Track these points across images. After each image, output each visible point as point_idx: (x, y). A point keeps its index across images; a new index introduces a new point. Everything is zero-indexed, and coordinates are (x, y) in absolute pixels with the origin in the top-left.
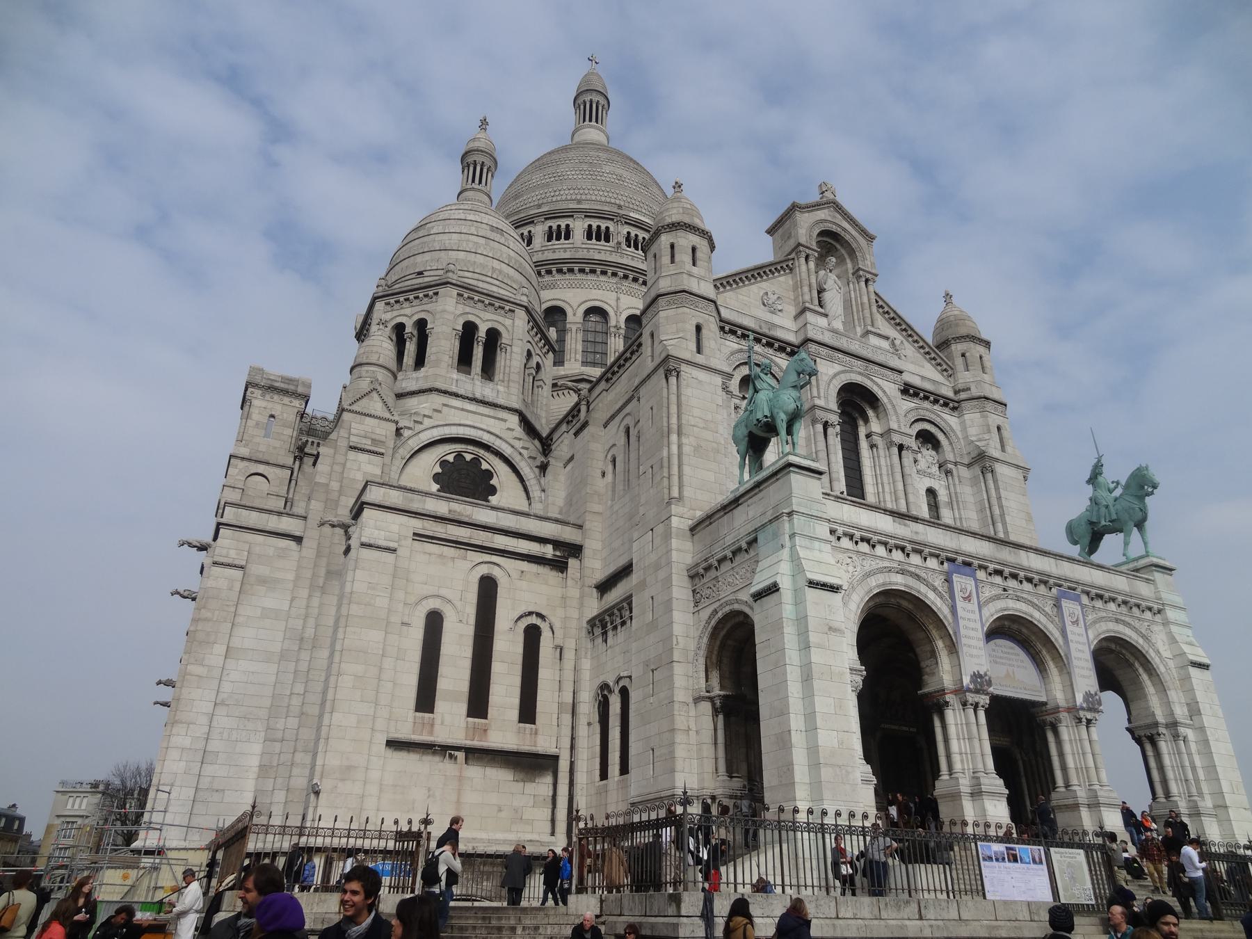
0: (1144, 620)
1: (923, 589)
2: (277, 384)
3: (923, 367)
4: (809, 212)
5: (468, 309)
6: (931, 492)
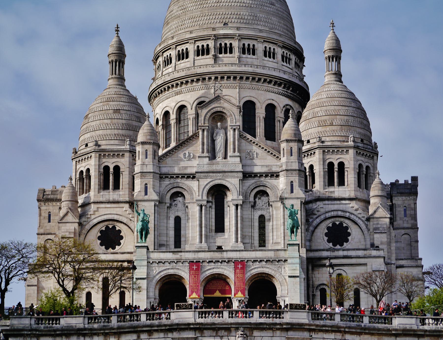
0: (277, 265)
2: (49, 197)
3: (266, 159)
4: (205, 107)
5: (104, 160)
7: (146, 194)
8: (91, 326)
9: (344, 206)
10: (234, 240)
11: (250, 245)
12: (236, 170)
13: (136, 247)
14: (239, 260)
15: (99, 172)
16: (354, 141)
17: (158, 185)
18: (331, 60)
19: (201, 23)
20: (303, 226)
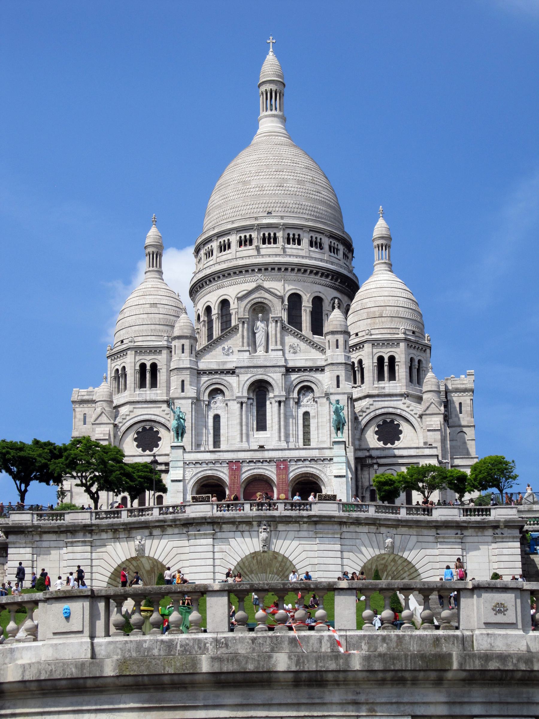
1: (219, 473)
3: (310, 352)
5: (141, 357)
6: (306, 414)
7: (183, 391)
8: (98, 522)
9: (395, 402)
10: (277, 439)
11: (293, 444)
12: (278, 364)
13: (171, 447)
14: (282, 460)
15: (135, 370)
16: (405, 333)
17: (196, 380)
18: (380, 248)
19: (244, 212)
20: (350, 423)
